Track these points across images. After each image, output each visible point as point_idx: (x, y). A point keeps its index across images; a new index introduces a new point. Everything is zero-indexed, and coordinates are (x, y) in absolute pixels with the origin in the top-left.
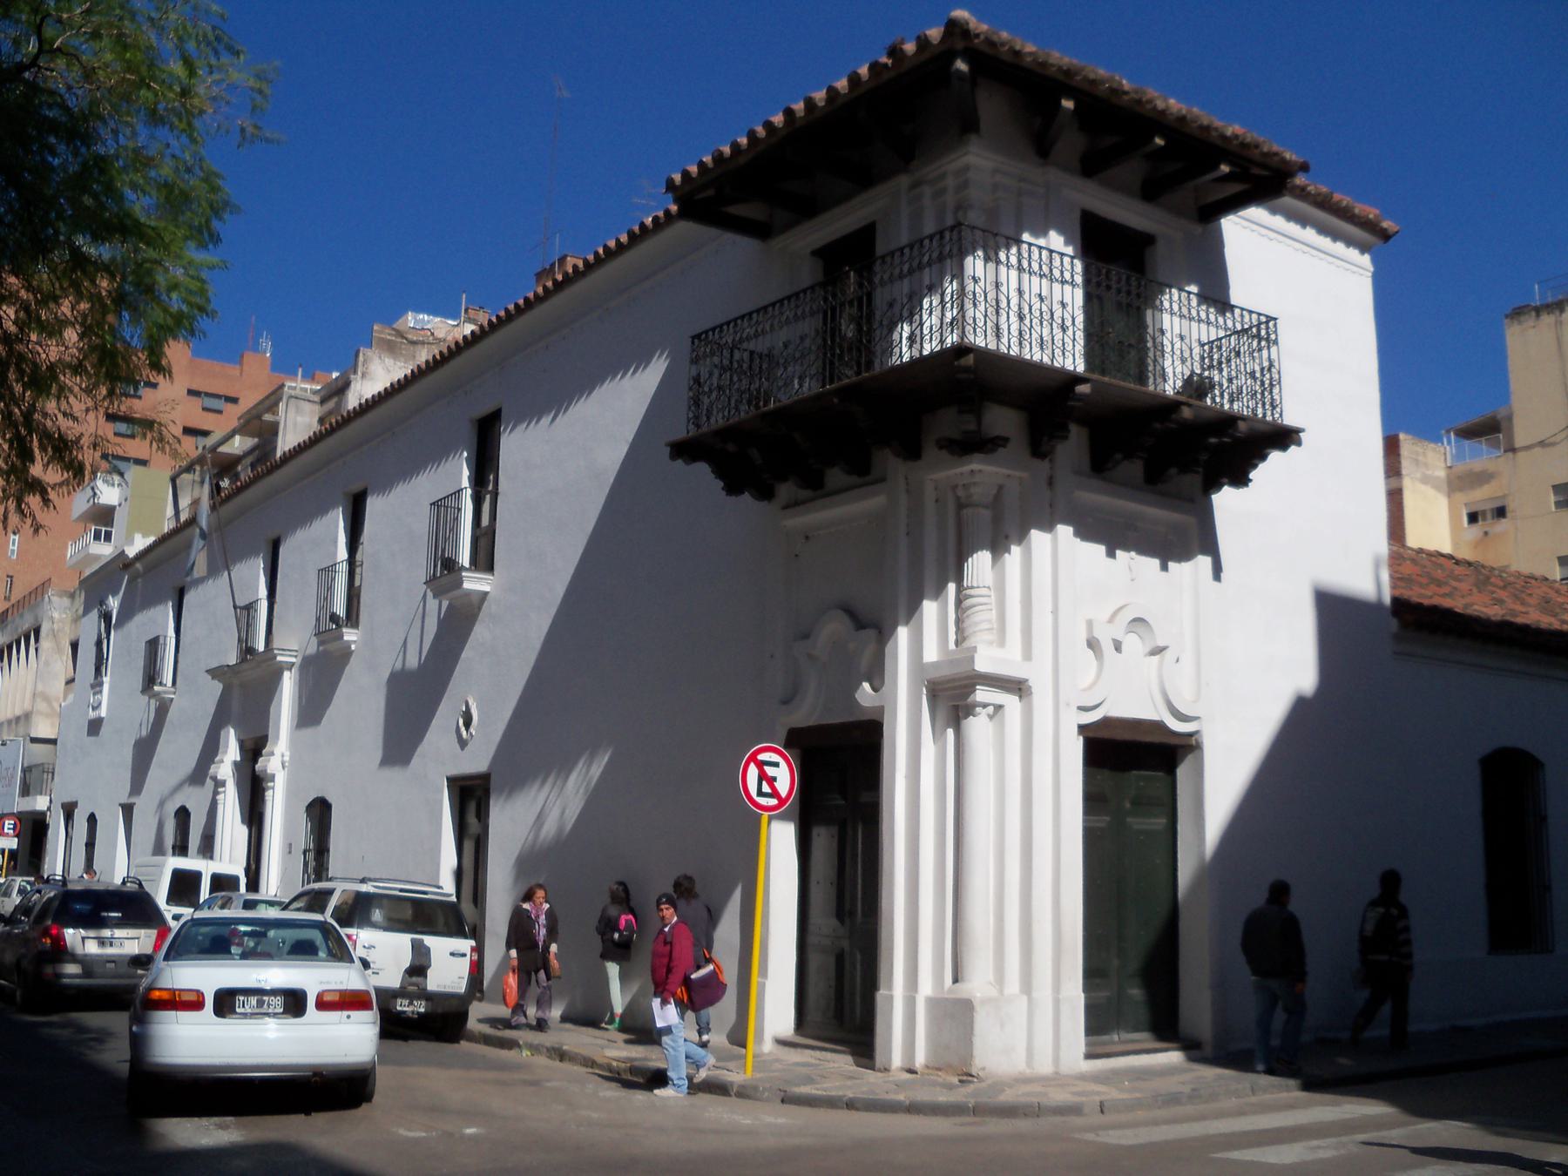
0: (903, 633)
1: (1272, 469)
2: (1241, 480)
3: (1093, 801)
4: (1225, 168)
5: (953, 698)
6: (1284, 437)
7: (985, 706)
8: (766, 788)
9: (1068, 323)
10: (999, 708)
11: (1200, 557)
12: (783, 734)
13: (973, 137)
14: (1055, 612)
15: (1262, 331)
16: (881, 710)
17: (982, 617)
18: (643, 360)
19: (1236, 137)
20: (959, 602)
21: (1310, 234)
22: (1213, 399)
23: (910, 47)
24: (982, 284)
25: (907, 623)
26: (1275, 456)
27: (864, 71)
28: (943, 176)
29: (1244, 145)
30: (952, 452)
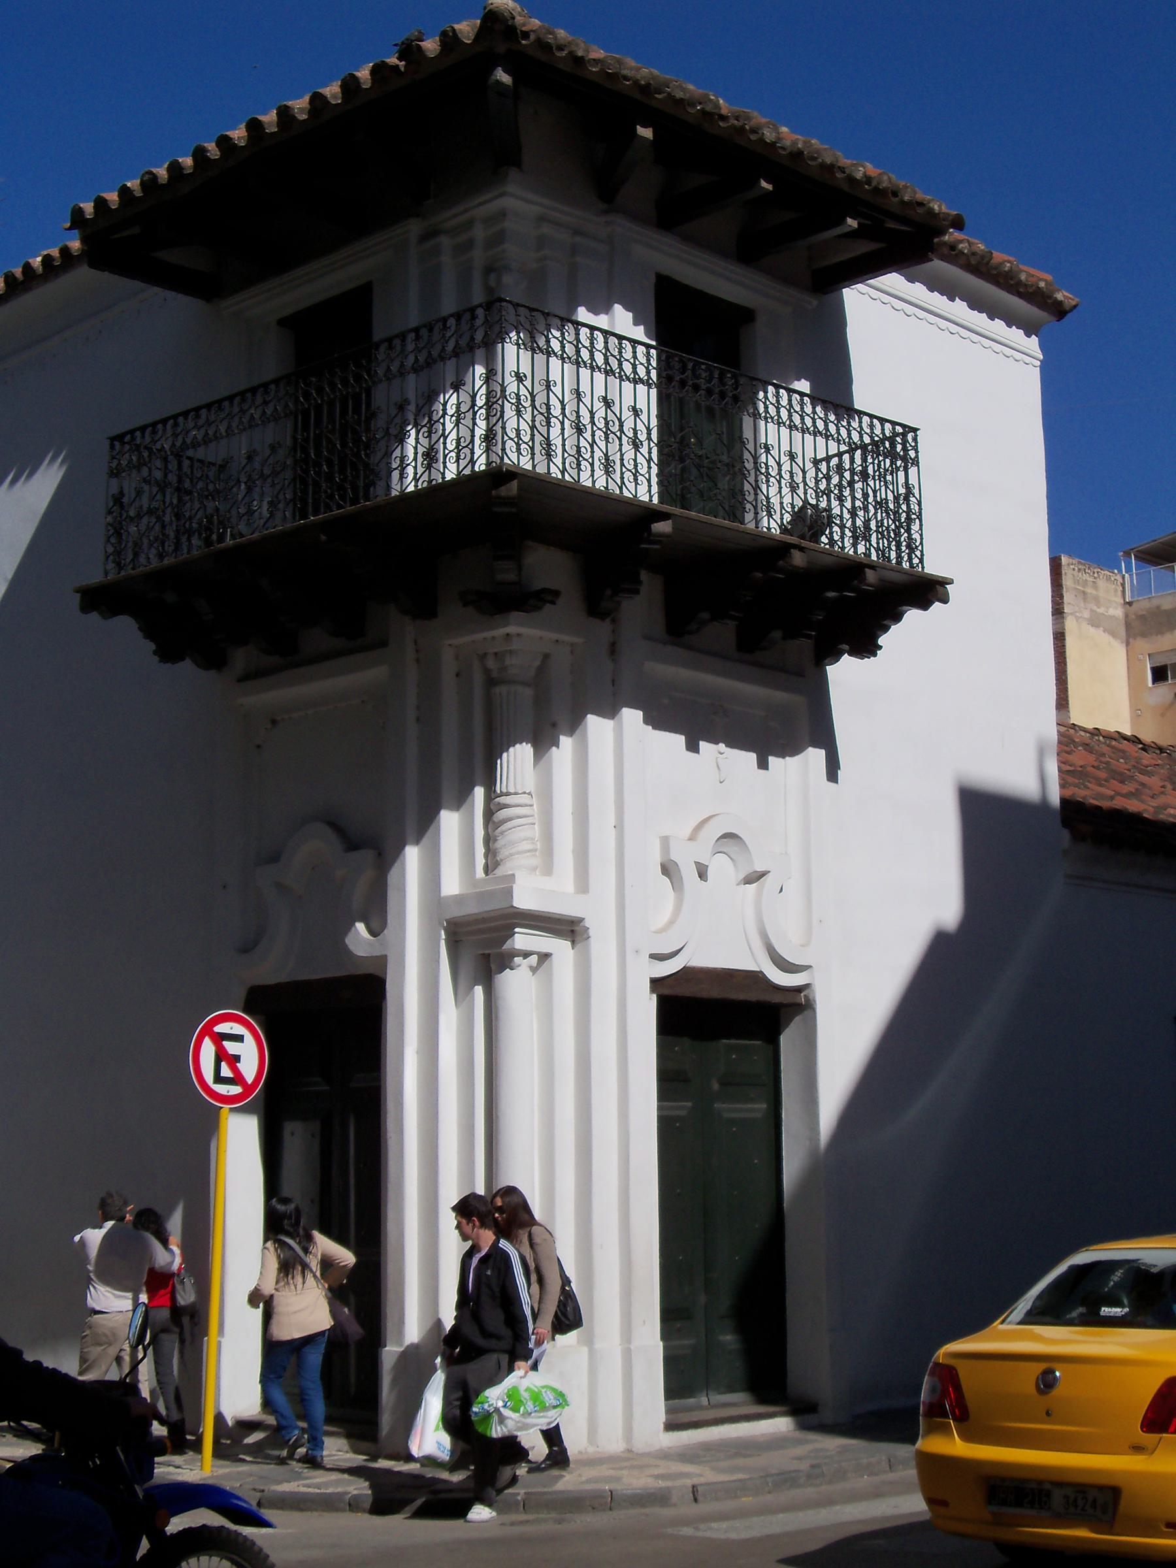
0: (412, 855)
2: (866, 647)
3: (670, 1080)
4: (852, 223)
5: (482, 944)
6: (927, 591)
7: (526, 955)
8: (226, 1071)
10: (544, 957)
11: (811, 750)
12: (241, 994)
13: (513, 173)
14: (619, 827)
15: (896, 446)
16: (382, 961)
17: (520, 836)
18: (28, 466)
19: (868, 179)
20: (489, 814)
21: (959, 309)
22: (831, 539)
23: (431, 46)
24: (528, 383)
25: (417, 842)
26: (912, 615)
27: (364, 74)
28: (470, 223)
29: (877, 191)
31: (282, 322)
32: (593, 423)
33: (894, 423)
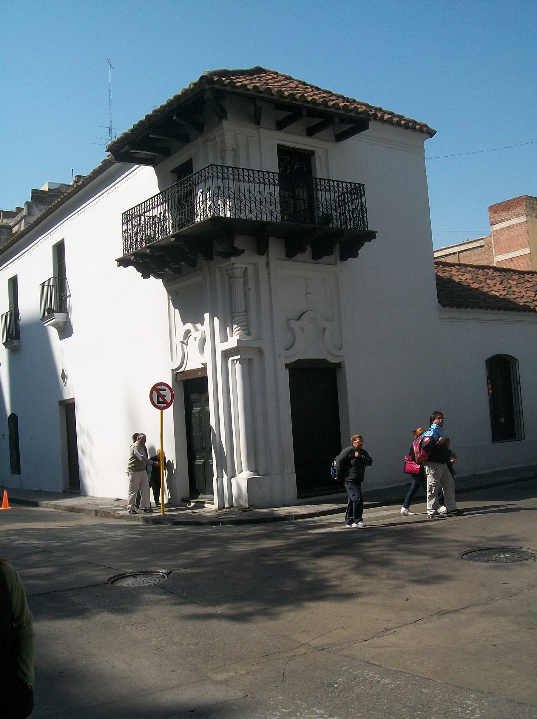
1: (367, 249)
8: (161, 400)
9: (263, 200)
13: (224, 122)
24: (222, 189)
26: (367, 243)
28: (215, 138)
30: (222, 257)
31: (171, 172)
32: (245, 198)
33: (355, 184)
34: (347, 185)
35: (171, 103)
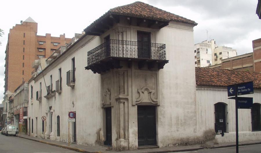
1: (166, 66)
6: (167, 62)
9: (128, 50)
10: (124, 102)
34: (159, 45)
35: (100, 18)
